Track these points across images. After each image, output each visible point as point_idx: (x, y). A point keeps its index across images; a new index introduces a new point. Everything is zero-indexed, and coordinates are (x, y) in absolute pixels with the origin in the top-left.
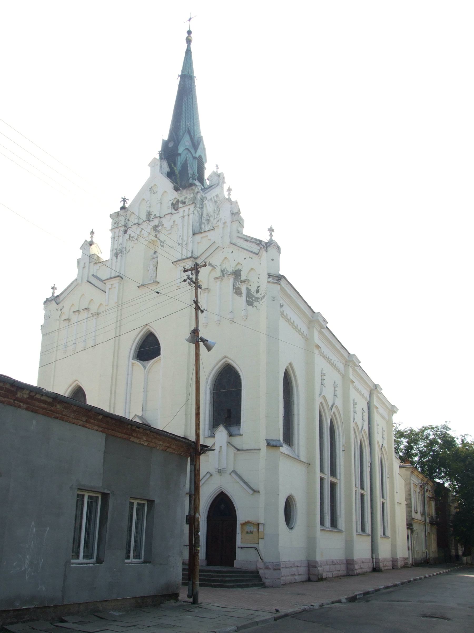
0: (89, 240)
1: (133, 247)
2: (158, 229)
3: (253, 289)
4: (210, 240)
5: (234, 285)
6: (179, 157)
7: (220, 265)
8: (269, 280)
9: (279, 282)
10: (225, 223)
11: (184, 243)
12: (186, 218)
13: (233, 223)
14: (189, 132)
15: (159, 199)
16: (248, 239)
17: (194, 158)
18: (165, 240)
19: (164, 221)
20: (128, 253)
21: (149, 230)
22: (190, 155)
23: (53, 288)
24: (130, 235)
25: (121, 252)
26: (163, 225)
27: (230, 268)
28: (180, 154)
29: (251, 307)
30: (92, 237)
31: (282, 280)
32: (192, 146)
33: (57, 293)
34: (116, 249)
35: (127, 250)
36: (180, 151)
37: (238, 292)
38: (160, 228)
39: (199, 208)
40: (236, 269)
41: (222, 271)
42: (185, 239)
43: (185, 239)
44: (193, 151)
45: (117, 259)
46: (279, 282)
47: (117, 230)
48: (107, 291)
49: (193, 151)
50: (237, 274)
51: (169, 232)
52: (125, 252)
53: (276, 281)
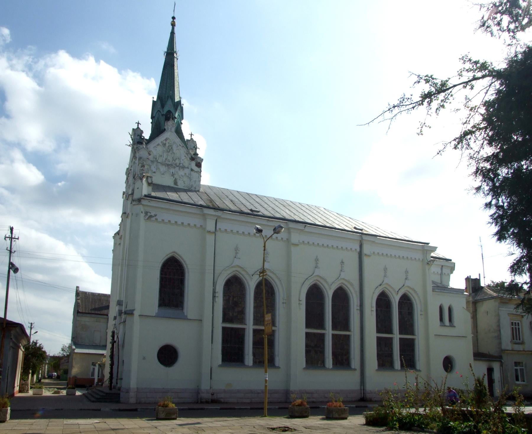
17: (162, 115)
44: (161, 111)
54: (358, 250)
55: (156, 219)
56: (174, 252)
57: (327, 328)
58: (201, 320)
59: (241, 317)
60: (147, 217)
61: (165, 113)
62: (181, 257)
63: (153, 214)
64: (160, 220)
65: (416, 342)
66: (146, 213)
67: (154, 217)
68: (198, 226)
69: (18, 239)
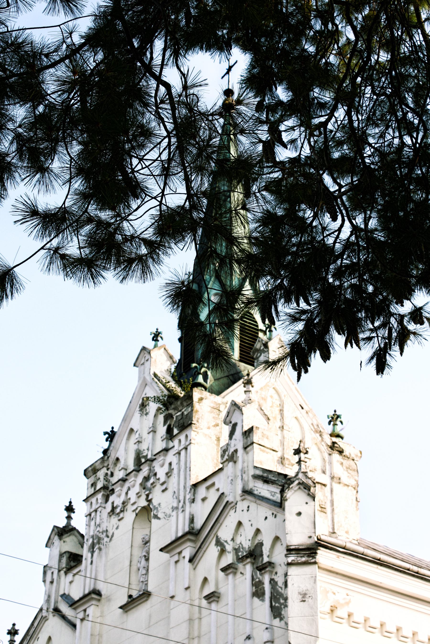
0: (62, 523)
1: (117, 528)
2: (149, 484)
3: (280, 581)
4: (218, 490)
5: (253, 579)
7: (233, 540)
8: (290, 560)
9: (314, 557)
11: (181, 504)
12: (183, 453)
13: (248, 449)
15: (151, 425)
16: (271, 477)
18: (159, 504)
19: (156, 464)
20: (111, 540)
21: (137, 488)
23: (9, 633)
24: (113, 503)
25: (99, 540)
26: (155, 474)
29: (278, 619)
30: (69, 518)
31: (318, 551)
34: (93, 537)
35: (110, 535)
38: (152, 480)
40: (256, 542)
41: (237, 550)
42: (181, 498)
43: (181, 498)
45: (92, 556)
47: (94, 500)
48: (78, 623)
50: (254, 554)
51: (164, 487)
52: (106, 539)
64: (358, 617)
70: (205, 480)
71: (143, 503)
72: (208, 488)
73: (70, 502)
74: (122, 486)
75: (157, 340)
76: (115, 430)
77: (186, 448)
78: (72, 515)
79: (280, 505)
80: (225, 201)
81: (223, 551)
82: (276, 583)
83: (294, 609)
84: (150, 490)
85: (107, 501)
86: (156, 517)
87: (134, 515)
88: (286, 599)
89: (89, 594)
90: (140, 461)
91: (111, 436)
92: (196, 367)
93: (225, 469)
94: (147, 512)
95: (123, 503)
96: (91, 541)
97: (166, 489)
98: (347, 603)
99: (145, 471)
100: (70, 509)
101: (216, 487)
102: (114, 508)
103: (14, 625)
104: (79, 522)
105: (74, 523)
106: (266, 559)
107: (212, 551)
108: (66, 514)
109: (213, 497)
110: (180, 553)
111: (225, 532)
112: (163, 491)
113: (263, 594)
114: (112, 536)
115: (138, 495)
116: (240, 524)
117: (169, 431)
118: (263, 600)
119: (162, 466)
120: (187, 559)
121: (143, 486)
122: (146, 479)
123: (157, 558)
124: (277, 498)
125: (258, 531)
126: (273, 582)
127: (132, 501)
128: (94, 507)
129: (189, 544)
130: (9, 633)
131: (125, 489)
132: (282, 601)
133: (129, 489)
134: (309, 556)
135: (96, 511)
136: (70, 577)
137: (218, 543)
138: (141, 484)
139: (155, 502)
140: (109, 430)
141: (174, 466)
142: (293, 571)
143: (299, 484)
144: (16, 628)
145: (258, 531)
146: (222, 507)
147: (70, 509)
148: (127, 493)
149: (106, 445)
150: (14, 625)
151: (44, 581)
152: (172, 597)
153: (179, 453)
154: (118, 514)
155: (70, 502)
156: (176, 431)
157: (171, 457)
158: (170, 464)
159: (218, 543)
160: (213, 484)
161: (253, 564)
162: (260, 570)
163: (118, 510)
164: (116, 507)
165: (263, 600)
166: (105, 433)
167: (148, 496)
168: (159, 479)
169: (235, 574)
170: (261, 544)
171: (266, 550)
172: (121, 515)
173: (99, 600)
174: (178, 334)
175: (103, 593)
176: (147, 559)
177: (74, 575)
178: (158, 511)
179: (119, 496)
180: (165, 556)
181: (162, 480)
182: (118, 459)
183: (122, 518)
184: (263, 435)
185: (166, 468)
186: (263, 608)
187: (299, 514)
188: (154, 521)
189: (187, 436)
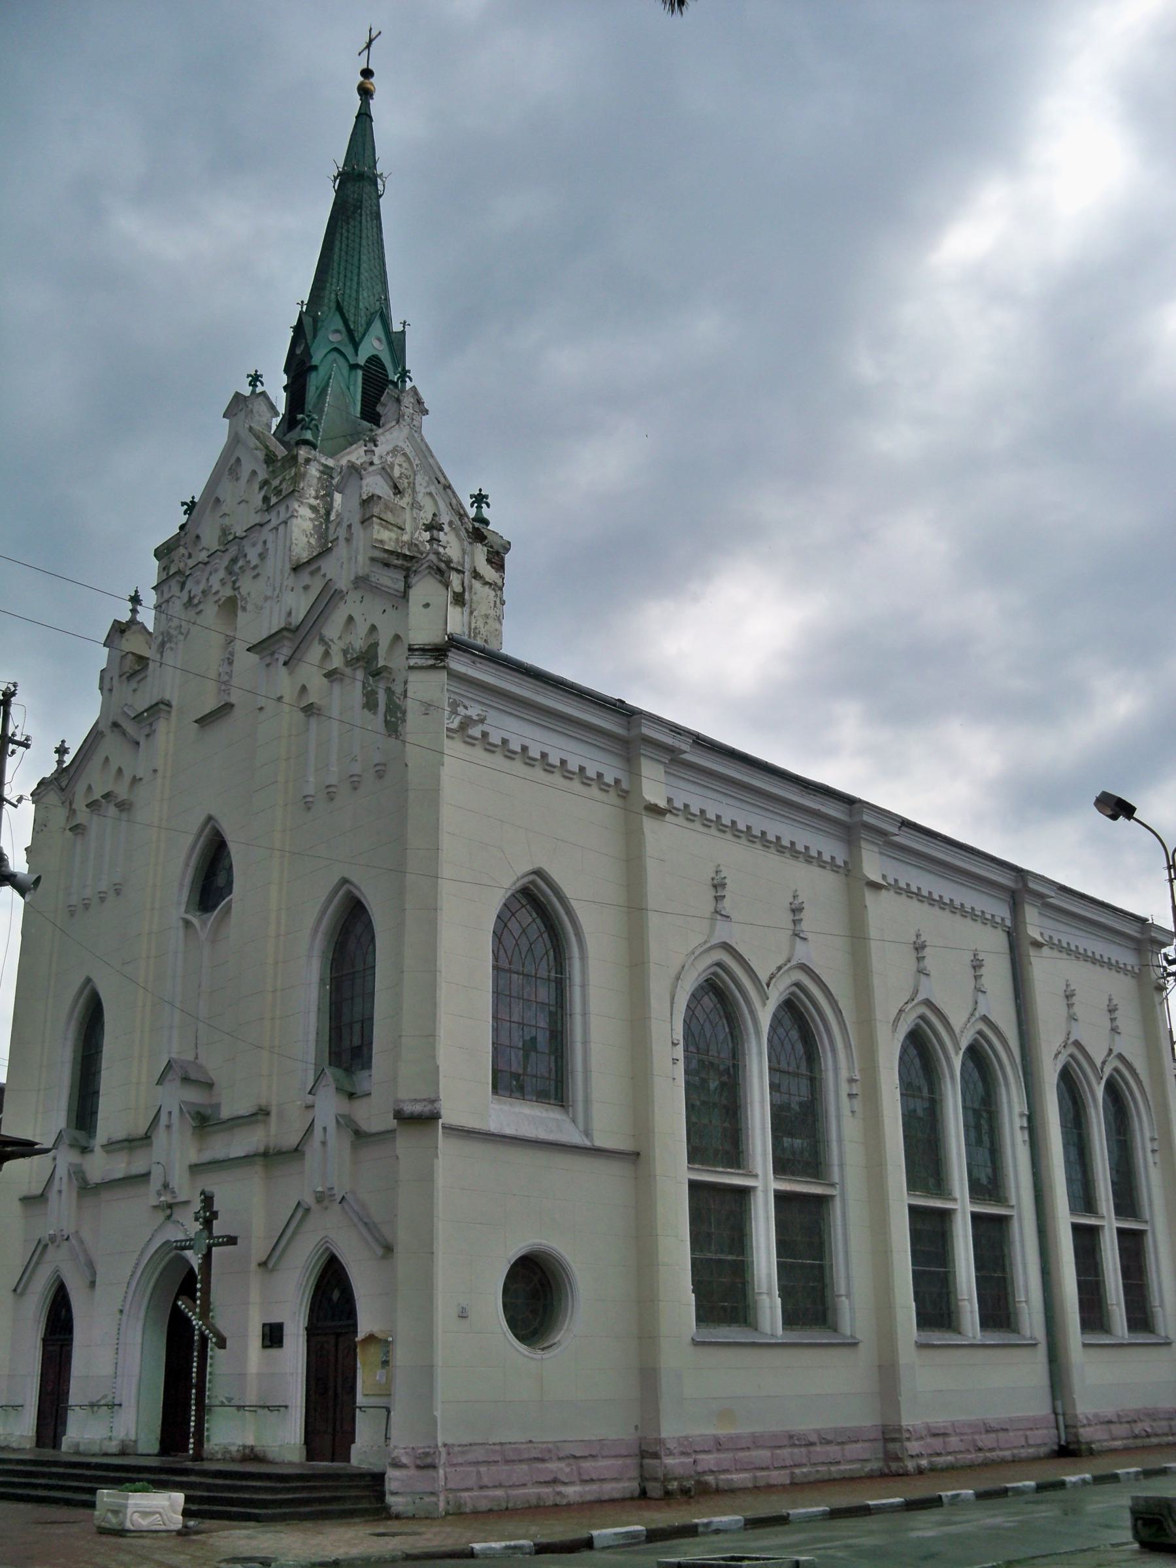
0: (125, 617)
2: (236, 568)
3: (398, 689)
6: (313, 375)
7: (340, 638)
8: (412, 662)
10: (350, 526)
11: (277, 592)
12: (282, 528)
14: (339, 308)
17: (354, 367)
21: (222, 574)
22: (341, 361)
23: (58, 751)
26: (245, 556)
27: (358, 642)
28: (315, 368)
32: (346, 340)
33: (68, 759)
34: (162, 634)
36: (315, 361)
37: (370, 704)
38: (241, 563)
39: (316, 498)
41: (345, 652)
42: (278, 585)
46: (442, 661)
48: (142, 741)
49: (348, 350)
51: (255, 573)
53: (431, 662)
54: (1008, 923)
55: (485, 735)
56: (539, 873)
57: (957, 1193)
58: (638, 1154)
59: (733, 1152)
60: (455, 725)
61: (361, 361)
62: (889, 856)
63: (474, 711)
64: (495, 738)
65: (1149, 1240)
66: (454, 705)
67: (476, 722)
68: (609, 779)
69: (27, 746)
70: (308, 562)
71: (228, 592)
72: (312, 573)
73: (136, 592)
74: (203, 571)
75: (255, 386)
76: (196, 500)
77: (285, 522)
78: (139, 608)
79: (405, 596)
80: (354, 212)
81: (327, 654)
82: (393, 693)
83: (414, 721)
84: (237, 575)
85: (182, 589)
86: (244, 609)
87: (216, 608)
88: (404, 713)
89: (157, 704)
90: (228, 539)
91: (190, 507)
92: (303, 419)
93: (335, 550)
94: (231, 606)
95: (203, 592)
96: (160, 639)
97: (258, 575)
98: (482, 721)
99: (233, 550)
100: (135, 600)
101: (322, 572)
102: (191, 599)
103: (63, 742)
104: (147, 617)
105: (139, 618)
106: (381, 663)
107: (317, 651)
108: (130, 605)
109: (317, 586)
110: (273, 654)
111: (333, 629)
112: (255, 577)
113: (376, 706)
114: (188, 633)
115: (223, 582)
116: (350, 619)
117: (266, 499)
118: (375, 713)
119: (254, 545)
120: (281, 661)
121: (229, 571)
122: (234, 561)
123: (246, 661)
124: (401, 586)
125: (373, 628)
126: (389, 692)
127: (214, 591)
128: (166, 596)
129: (286, 643)
130: (58, 751)
131: (206, 574)
132: (399, 715)
133: (211, 574)
134: (436, 659)
135: (167, 601)
136: (134, 685)
137: (322, 640)
138: (227, 568)
139: (243, 591)
140: (188, 500)
141: (269, 545)
142: (414, 677)
143: (429, 567)
144: (66, 746)
145: (373, 628)
146: (329, 598)
147: (135, 600)
148: (208, 580)
149: (184, 519)
150: (63, 742)
151: (101, 689)
152: (261, 709)
153: (276, 528)
154: (196, 605)
155: (136, 592)
156: (274, 500)
157: (266, 534)
158: (265, 542)
159: (322, 640)
160: (319, 569)
161: (365, 668)
162: (373, 676)
163: (196, 601)
164: (194, 597)
165: (375, 713)
166: (183, 504)
167: (234, 582)
168: (249, 562)
169: (342, 680)
170: (376, 644)
171: (382, 651)
172: (200, 607)
173: (169, 712)
174: (284, 379)
175: (174, 703)
176: (231, 663)
177: (139, 682)
178: (246, 602)
179: (198, 583)
180: (253, 658)
181: (253, 563)
182: (198, 537)
183: (201, 611)
184: (387, 507)
185: (259, 548)
186: (377, 721)
187: (427, 605)
188: (240, 613)
189: (287, 507)
